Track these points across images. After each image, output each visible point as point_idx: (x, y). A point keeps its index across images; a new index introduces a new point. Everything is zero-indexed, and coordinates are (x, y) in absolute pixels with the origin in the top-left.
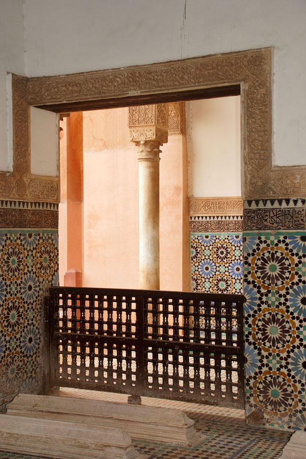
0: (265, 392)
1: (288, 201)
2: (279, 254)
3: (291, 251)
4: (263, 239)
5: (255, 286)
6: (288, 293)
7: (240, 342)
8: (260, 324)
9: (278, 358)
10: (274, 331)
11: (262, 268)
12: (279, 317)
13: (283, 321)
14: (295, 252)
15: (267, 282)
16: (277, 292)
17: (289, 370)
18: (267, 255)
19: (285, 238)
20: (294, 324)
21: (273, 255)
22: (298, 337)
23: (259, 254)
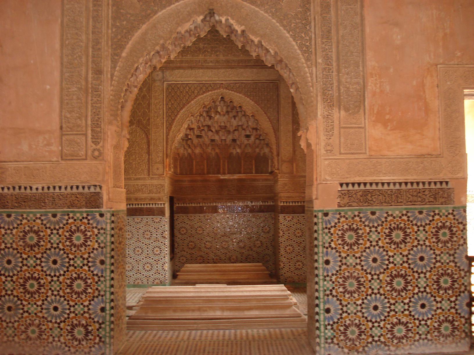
22: (4, 288)
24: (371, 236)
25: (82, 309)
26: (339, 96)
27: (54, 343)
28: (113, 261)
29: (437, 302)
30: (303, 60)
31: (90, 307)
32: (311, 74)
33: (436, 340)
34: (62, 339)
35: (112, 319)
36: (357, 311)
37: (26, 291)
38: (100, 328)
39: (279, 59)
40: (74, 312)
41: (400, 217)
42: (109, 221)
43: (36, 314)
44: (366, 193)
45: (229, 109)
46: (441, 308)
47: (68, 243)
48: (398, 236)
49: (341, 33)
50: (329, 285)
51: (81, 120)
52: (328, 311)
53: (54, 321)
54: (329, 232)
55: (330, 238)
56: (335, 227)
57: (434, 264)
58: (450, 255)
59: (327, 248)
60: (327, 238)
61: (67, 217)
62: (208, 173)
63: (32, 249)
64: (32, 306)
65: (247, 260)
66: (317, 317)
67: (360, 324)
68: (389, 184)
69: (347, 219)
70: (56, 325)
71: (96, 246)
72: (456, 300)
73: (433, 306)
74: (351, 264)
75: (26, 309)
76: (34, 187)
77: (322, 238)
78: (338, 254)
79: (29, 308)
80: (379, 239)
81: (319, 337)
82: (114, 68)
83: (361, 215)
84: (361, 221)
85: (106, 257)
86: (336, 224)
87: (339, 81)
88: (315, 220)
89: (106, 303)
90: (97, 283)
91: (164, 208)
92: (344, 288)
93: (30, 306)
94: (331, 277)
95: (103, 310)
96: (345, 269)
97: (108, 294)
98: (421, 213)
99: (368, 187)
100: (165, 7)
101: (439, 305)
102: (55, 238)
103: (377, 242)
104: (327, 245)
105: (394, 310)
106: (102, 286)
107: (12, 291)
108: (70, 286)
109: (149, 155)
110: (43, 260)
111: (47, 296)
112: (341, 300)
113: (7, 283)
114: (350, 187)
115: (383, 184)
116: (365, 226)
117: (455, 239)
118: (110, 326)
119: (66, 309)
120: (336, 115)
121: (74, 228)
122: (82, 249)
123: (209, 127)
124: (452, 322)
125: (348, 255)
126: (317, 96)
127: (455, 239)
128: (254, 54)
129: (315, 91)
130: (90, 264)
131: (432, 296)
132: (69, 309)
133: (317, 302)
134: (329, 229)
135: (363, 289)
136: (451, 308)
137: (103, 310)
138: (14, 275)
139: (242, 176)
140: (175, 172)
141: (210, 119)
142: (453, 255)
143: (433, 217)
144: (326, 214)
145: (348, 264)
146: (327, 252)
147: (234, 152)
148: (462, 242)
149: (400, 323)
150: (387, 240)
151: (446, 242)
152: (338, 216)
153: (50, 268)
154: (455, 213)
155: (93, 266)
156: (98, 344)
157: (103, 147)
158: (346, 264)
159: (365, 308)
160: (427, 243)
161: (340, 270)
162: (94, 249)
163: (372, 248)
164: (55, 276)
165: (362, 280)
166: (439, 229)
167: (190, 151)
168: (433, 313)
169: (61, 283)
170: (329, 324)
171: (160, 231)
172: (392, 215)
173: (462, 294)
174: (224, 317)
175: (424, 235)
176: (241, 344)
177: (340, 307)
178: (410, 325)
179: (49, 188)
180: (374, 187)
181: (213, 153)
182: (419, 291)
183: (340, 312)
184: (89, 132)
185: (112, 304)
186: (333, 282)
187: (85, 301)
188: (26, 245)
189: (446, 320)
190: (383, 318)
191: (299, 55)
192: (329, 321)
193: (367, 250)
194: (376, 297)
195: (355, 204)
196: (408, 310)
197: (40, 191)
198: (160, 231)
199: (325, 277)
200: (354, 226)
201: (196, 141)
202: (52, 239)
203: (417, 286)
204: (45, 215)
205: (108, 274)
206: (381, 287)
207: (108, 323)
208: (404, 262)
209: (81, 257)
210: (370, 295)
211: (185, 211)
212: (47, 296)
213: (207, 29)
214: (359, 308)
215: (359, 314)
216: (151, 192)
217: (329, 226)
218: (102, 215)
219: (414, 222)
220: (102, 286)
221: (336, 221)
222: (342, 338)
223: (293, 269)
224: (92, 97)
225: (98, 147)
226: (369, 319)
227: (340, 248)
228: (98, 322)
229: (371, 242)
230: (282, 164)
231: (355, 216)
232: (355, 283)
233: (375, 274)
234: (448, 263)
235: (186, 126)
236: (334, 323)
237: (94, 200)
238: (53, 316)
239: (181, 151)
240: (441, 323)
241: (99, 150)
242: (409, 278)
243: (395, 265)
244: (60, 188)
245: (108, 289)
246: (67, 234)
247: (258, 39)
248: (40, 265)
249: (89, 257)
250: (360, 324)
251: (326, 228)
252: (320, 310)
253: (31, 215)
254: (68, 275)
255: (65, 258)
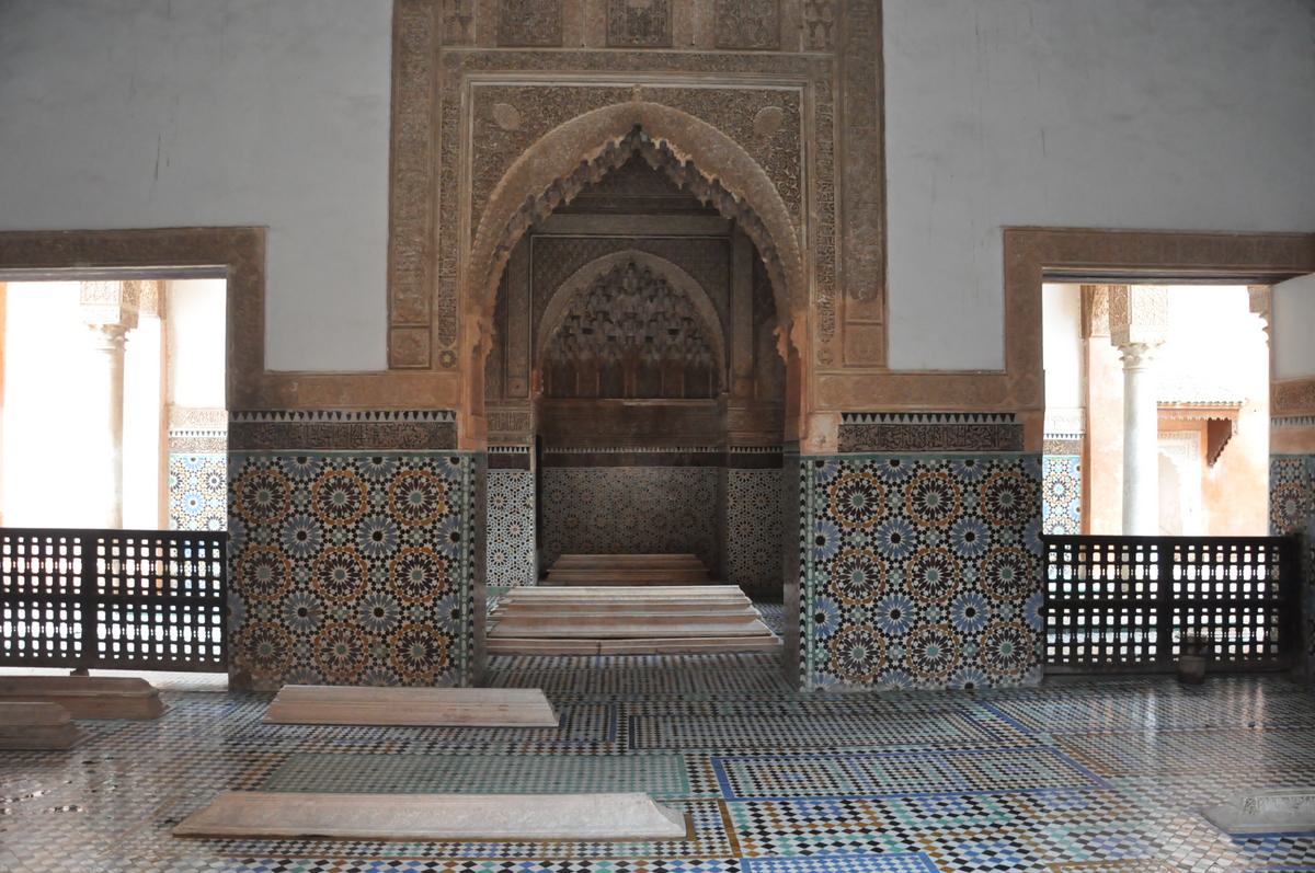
0: (252, 649)
1: (283, 415)
2: (271, 480)
3: (286, 475)
4: (252, 460)
5: (241, 520)
6: (281, 527)
7: (223, 590)
8: (247, 566)
9: (269, 607)
10: (264, 574)
11: (250, 496)
12: (271, 556)
13: (276, 561)
14: (290, 476)
15: (256, 514)
16: (269, 526)
17: (282, 620)
18: (256, 480)
19: (279, 459)
20: (289, 564)
21: (264, 480)
22: (293, 579)
23: (246, 480)
24: (890, 500)
25: (421, 613)
26: (844, 273)
27: (376, 669)
28: (472, 535)
29: (993, 607)
30: (786, 212)
31: (436, 609)
32: (799, 236)
33: (990, 666)
34: (389, 662)
35: (471, 629)
36: (867, 619)
37: (330, 583)
38: (452, 643)
39: (745, 208)
40: (409, 618)
41: (938, 470)
42: (466, 470)
43: (346, 621)
44: (883, 430)
45: (643, 284)
46: (998, 616)
47: (399, 505)
48: (932, 500)
49: (848, 169)
50: (822, 577)
51: (423, 304)
52: (820, 618)
53: (375, 632)
54: (824, 492)
55: (825, 501)
56: (833, 483)
57: (990, 545)
58: (1015, 532)
59: (820, 518)
60: (820, 501)
61: (397, 463)
62: (602, 396)
63: (339, 515)
64: (340, 608)
65: (669, 548)
66: (802, 628)
67: (871, 640)
68: (920, 416)
69: (852, 471)
70: (380, 639)
71: (446, 510)
72: (1023, 603)
73: (987, 612)
74: (858, 544)
75: (329, 613)
76: (344, 413)
77: (814, 502)
78: (837, 528)
79: (335, 612)
80: (904, 505)
81: (803, 659)
82: (476, 217)
83: (876, 466)
84: (875, 475)
85: (461, 528)
86: (835, 478)
87: (843, 248)
88: (803, 472)
89: (461, 603)
90: (446, 570)
91: (527, 456)
92: (845, 583)
93: (336, 608)
94: (825, 564)
95: (456, 614)
96: (848, 552)
97: (465, 588)
98: (970, 463)
99: (888, 420)
100: (561, 120)
101: (996, 611)
102: (378, 498)
103: (900, 509)
104: (820, 513)
105: (925, 618)
106: (456, 575)
107: (306, 583)
108: (403, 575)
109: (503, 363)
110: (358, 532)
111: (365, 592)
112: (841, 602)
113: (297, 570)
114: (859, 420)
115: (911, 416)
116: (882, 483)
117: (1023, 506)
118: (467, 640)
119: (396, 613)
120: (837, 303)
121: (409, 480)
122: (423, 515)
123: (606, 314)
124: (1015, 639)
125: (854, 530)
126: (808, 271)
127: (1023, 506)
128: (703, 199)
129: (805, 264)
130: (435, 540)
131: (985, 596)
132: (401, 613)
133: (803, 603)
134: (825, 487)
135: (876, 584)
136: (1015, 616)
137: (456, 614)
138: (310, 557)
139: (665, 402)
140: (545, 394)
141: (608, 300)
142: (1019, 532)
143: (989, 470)
144: (820, 464)
145: (854, 543)
146: (820, 524)
147: (648, 358)
148: (1034, 511)
149: (933, 638)
150: (916, 507)
151: (1007, 512)
152: (839, 467)
153: (368, 546)
154: (1023, 465)
155: (439, 543)
156: (448, 669)
157: (458, 348)
158: (849, 543)
159: (879, 615)
160: (979, 512)
161: (841, 553)
162: (441, 515)
163: (892, 519)
164: (378, 558)
165: (876, 569)
166: (998, 489)
167: (570, 356)
168: (986, 623)
169: (387, 570)
170: (821, 640)
171: (521, 496)
172: (924, 466)
173: (1032, 595)
174: (642, 634)
175: (974, 499)
176: (676, 675)
177: (839, 612)
178: (950, 643)
179: (368, 415)
180: (897, 420)
181: (612, 360)
182: (965, 589)
183: (840, 620)
184: (436, 323)
185: (472, 605)
186: (829, 573)
187: (428, 600)
188: (330, 507)
189: (1007, 636)
190: (907, 630)
191: (779, 204)
192: (821, 635)
193: (884, 522)
194: (896, 598)
195: (867, 447)
196: (947, 618)
197: (354, 419)
198: (521, 496)
199: (816, 564)
200: (865, 482)
201: (582, 339)
202: (373, 498)
203: (961, 580)
204: (361, 460)
205: (465, 556)
206: (905, 581)
207: (464, 636)
208: (941, 542)
209: (421, 528)
210: (888, 594)
211: (559, 461)
212: (365, 592)
213: (626, 155)
214: (869, 614)
215: (870, 624)
216: (505, 427)
217: (824, 482)
218: (455, 460)
219: (959, 478)
220: (456, 575)
221: (836, 474)
222: (841, 661)
223: (751, 563)
224: (441, 265)
225: (450, 348)
226: (885, 631)
227: (840, 518)
228: (448, 634)
229: (890, 509)
230: (734, 383)
231: (866, 467)
232: (865, 576)
233: (896, 560)
234: (1011, 545)
235: (566, 313)
236: (829, 637)
237: (443, 436)
238: (374, 624)
239: (556, 356)
240: (998, 641)
241: (451, 354)
242: (950, 568)
243: (928, 546)
244: (387, 414)
245: (465, 581)
246: (398, 491)
247: (714, 176)
248: (353, 541)
249: (435, 528)
250: (871, 640)
251: (820, 485)
252: (807, 617)
253: (339, 460)
254: (399, 557)
255: (394, 530)
